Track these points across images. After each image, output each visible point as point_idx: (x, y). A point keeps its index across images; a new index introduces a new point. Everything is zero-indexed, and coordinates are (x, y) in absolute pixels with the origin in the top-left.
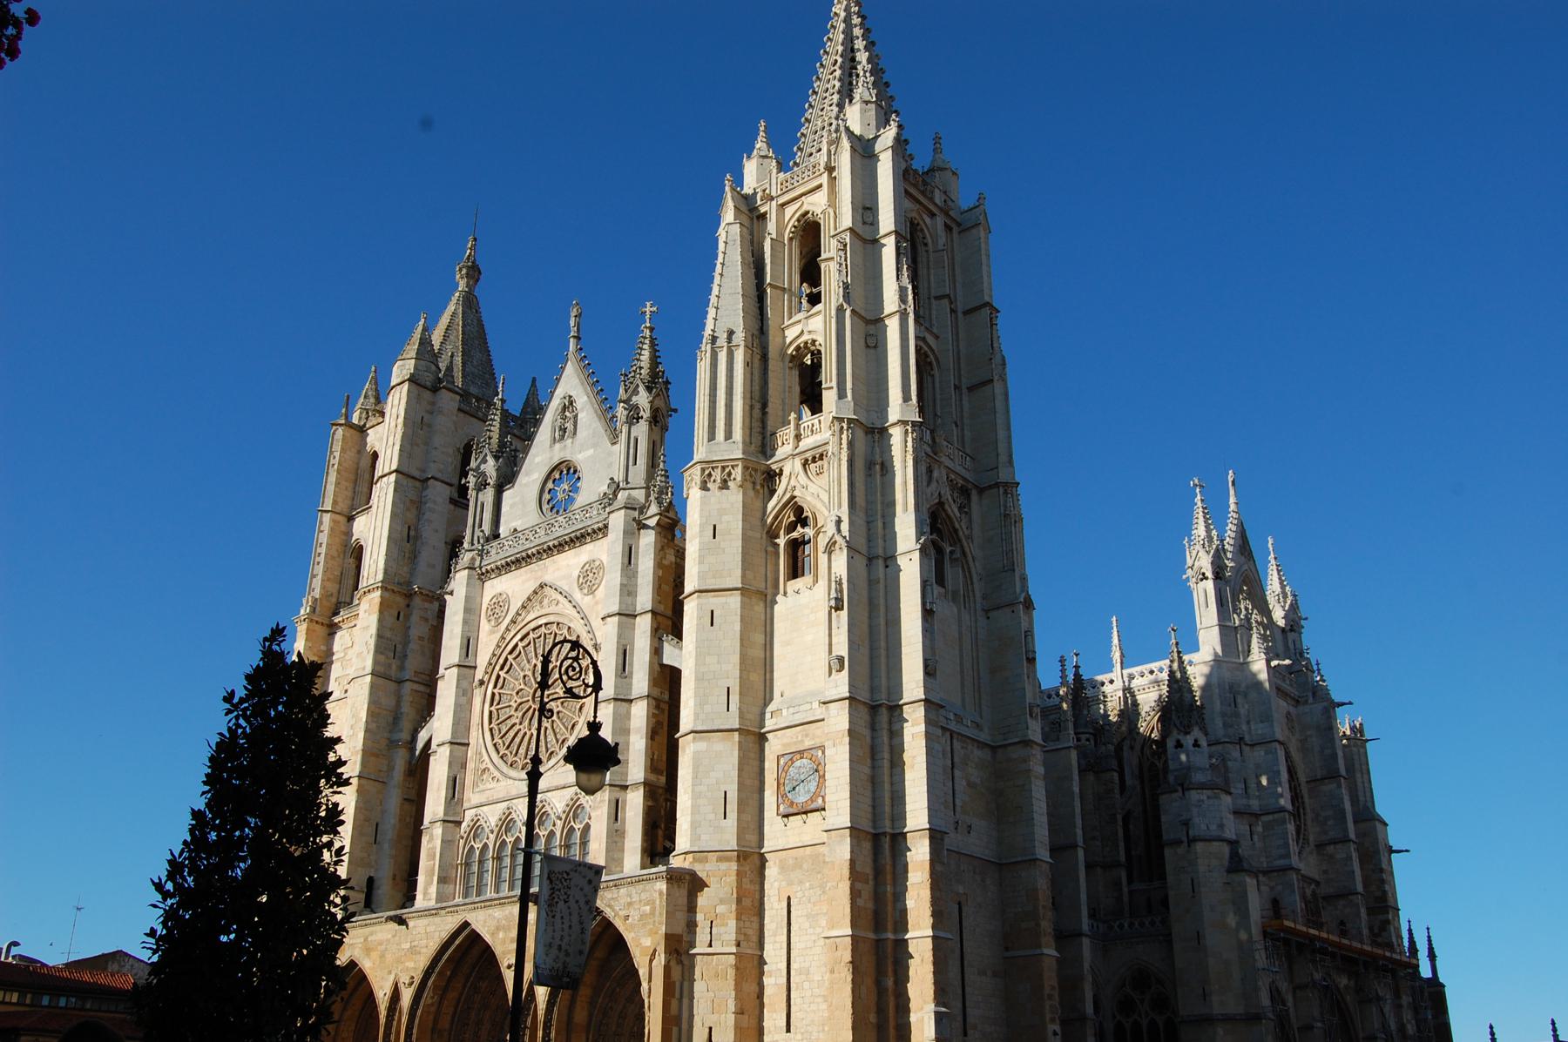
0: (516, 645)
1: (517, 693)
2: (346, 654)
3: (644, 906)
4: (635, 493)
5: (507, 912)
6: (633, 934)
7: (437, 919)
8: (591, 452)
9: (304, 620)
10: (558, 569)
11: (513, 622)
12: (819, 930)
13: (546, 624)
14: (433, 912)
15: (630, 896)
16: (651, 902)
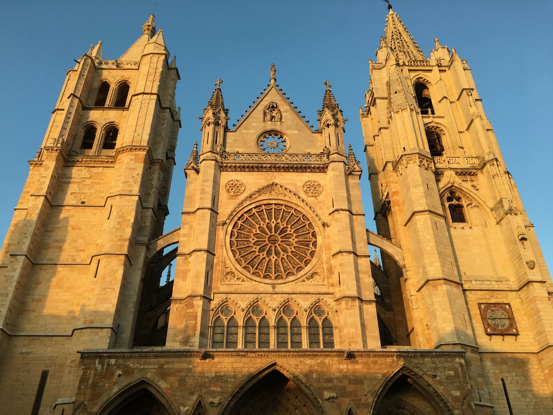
0: (251, 209)
1: (254, 235)
2: (84, 181)
3: (449, 370)
4: (343, 157)
5: (319, 361)
6: (442, 387)
7: (243, 360)
8: (297, 132)
9: (57, 150)
10: (285, 179)
11: (250, 197)
12: (528, 400)
13: (275, 204)
14: (243, 354)
15: (435, 363)
16: (456, 370)
